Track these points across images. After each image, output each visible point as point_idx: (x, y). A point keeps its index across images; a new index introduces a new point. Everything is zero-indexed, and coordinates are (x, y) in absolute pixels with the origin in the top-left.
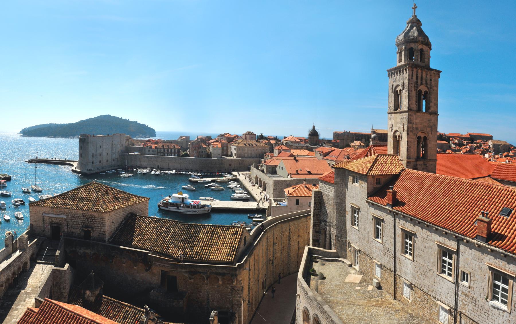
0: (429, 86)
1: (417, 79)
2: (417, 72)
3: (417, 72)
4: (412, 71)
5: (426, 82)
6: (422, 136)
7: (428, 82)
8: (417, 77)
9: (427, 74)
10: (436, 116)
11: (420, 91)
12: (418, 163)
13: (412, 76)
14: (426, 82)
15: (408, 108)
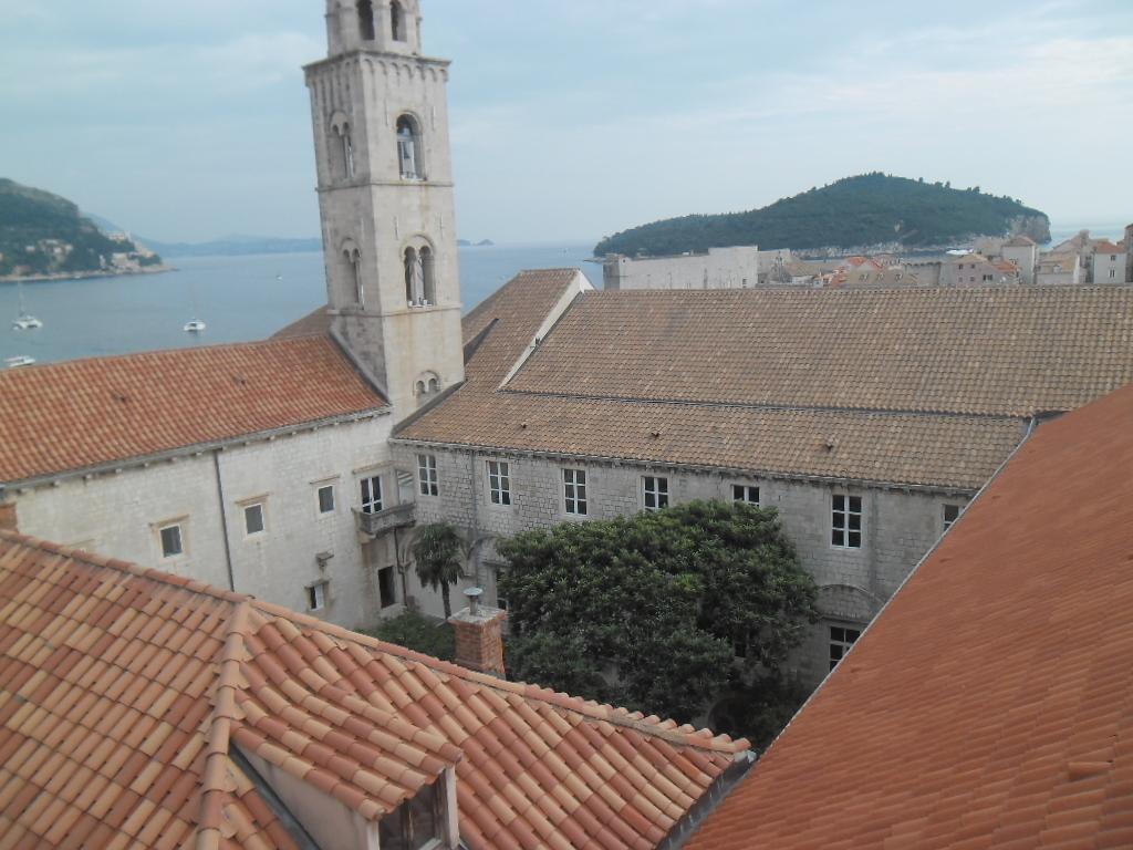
0: (346, 108)
1: (324, 100)
2: (322, 82)
3: (322, 82)
4: (314, 84)
5: (340, 97)
6: (350, 247)
7: (344, 94)
8: (324, 93)
9: (338, 77)
10: (367, 188)
11: (336, 128)
12: (349, 319)
13: (316, 96)
14: (340, 97)
15: (319, 182)
